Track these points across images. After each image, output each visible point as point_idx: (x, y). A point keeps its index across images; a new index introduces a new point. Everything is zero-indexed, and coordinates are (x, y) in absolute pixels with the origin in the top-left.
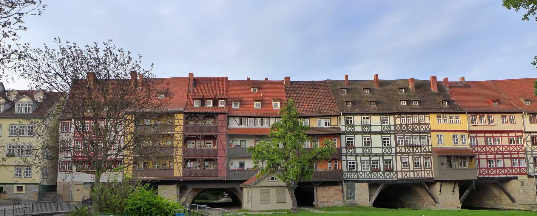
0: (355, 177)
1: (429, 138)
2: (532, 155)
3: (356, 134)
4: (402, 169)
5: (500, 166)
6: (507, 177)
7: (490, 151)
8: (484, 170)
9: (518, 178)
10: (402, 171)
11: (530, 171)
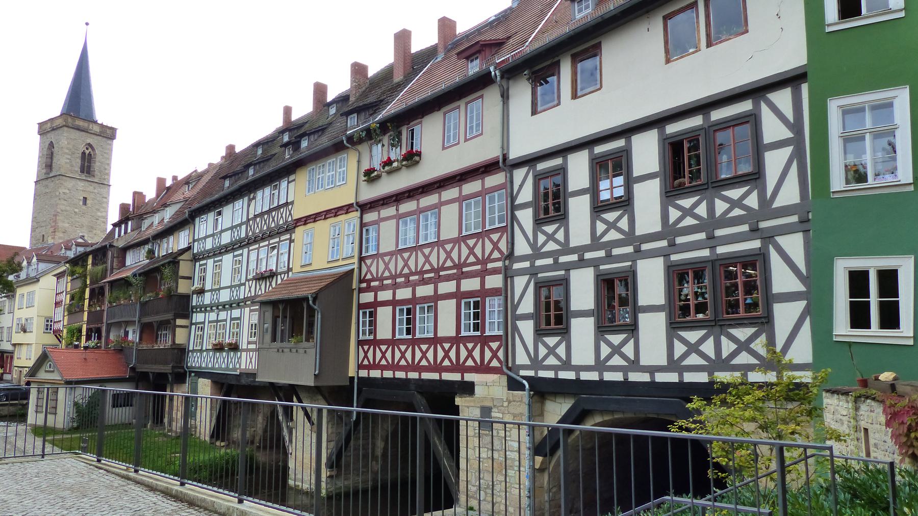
0: (197, 366)
1: (292, 244)
2: (532, 272)
3: (208, 256)
4: (249, 343)
5: (426, 335)
6: (441, 382)
7: (406, 271)
8: (384, 348)
9: (477, 389)
10: (247, 350)
11: (522, 358)
